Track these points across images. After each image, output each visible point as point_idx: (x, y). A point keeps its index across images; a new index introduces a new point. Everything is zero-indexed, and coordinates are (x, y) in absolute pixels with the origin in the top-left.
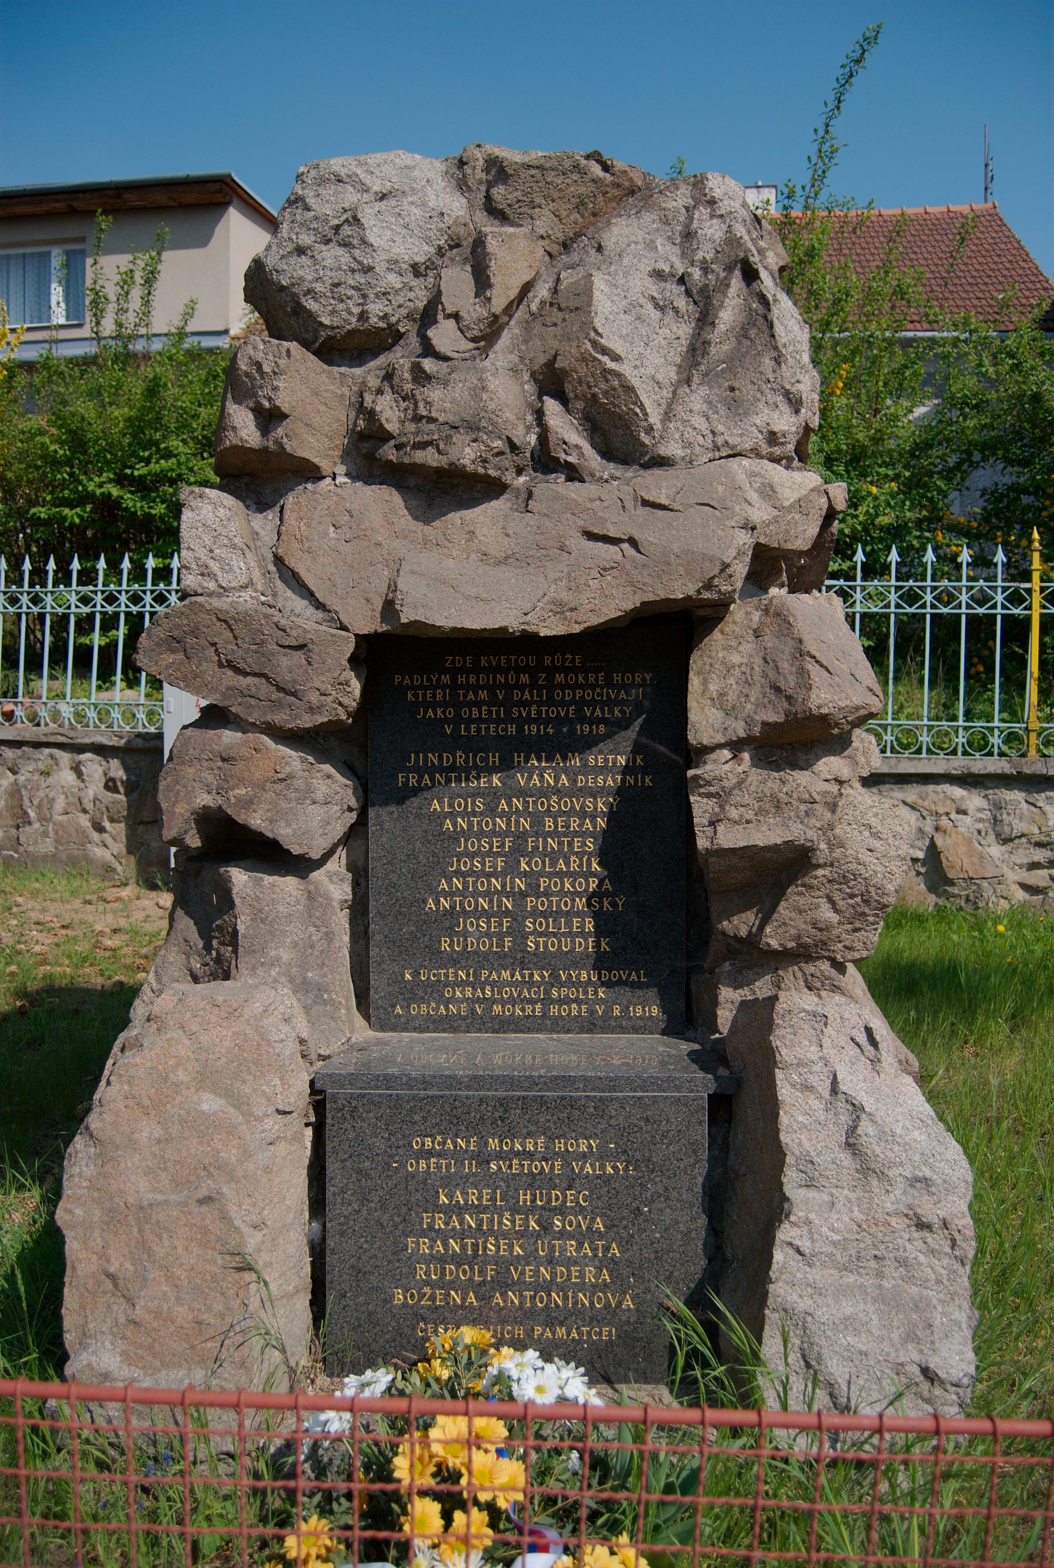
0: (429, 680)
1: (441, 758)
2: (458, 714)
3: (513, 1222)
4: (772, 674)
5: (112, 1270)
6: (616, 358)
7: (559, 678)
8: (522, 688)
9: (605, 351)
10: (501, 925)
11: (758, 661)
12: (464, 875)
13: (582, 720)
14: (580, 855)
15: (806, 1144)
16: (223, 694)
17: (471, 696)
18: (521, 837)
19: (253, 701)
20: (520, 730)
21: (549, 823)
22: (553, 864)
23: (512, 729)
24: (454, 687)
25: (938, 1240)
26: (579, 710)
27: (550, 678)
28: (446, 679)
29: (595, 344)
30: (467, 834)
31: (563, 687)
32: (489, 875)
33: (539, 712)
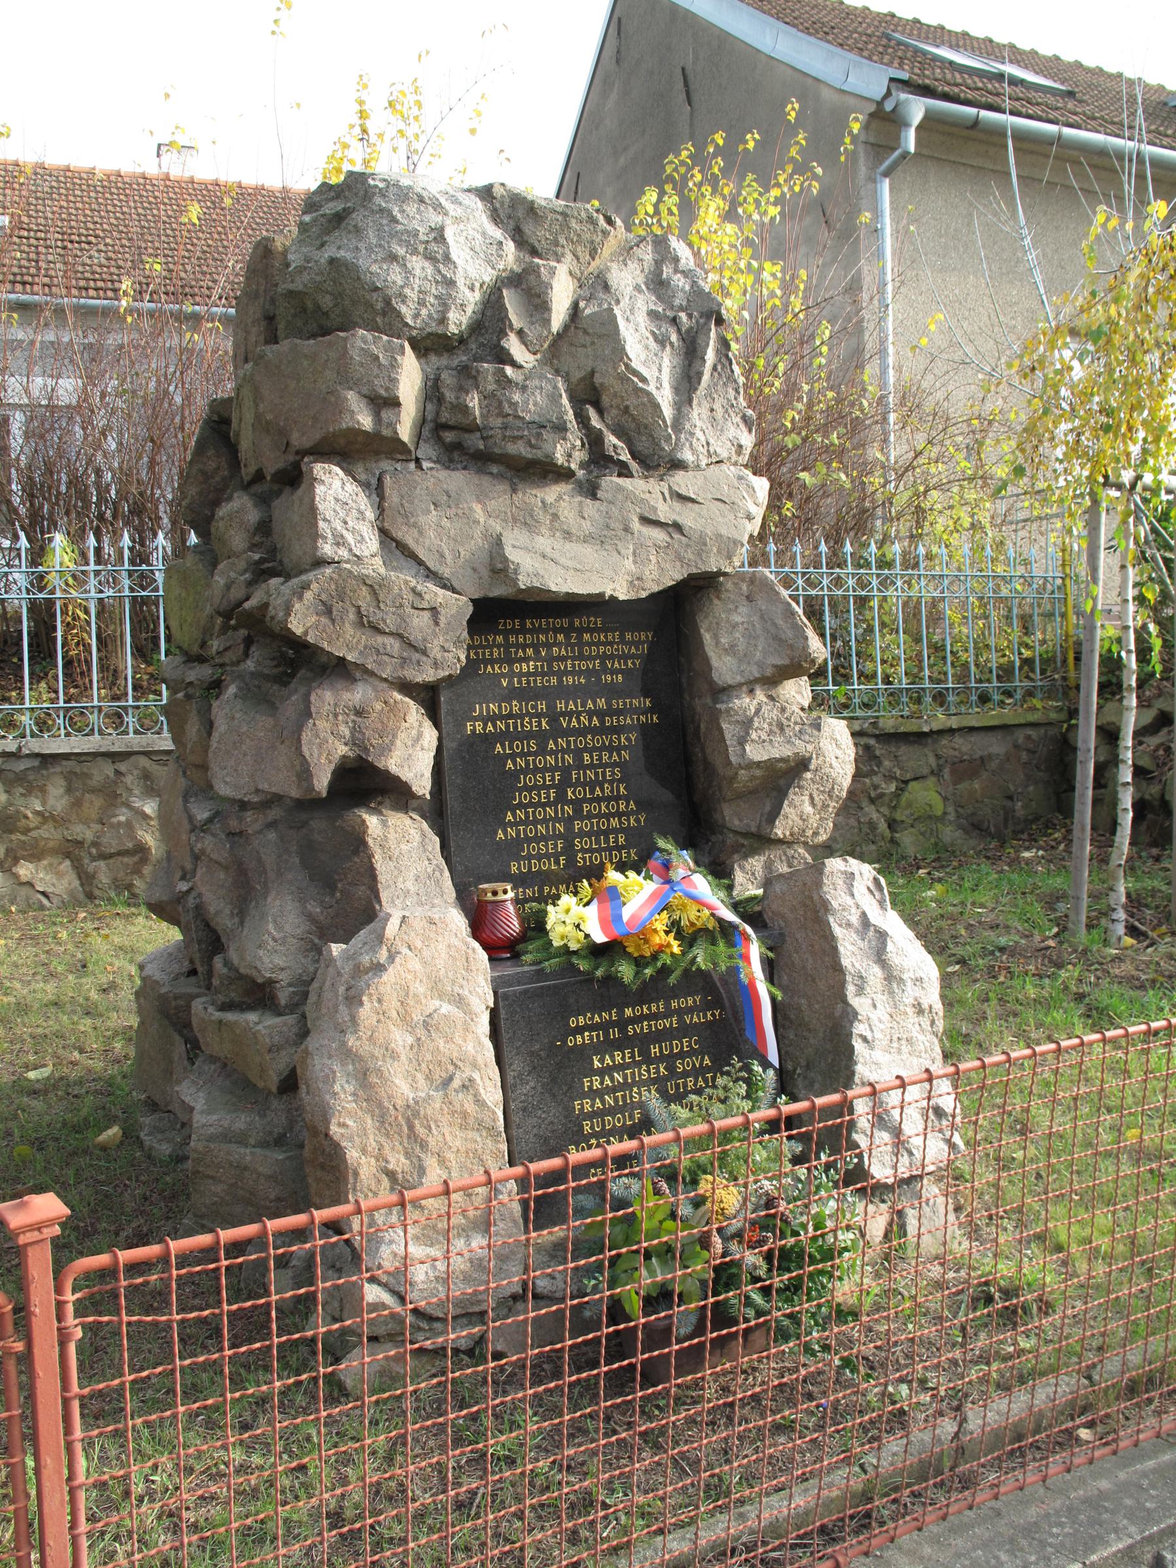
0: (487, 640)
1: (500, 707)
2: (511, 670)
3: (648, 1071)
4: (773, 630)
5: (391, 1167)
6: (644, 380)
7: (586, 637)
8: (559, 645)
9: (636, 373)
10: (556, 846)
11: (755, 618)
12: (526, 806)
13: (605, 670)
14: (611, 782)
15: (857, 965)
16: (361, 653)
17: (521, 654)
18: (566, 771)
19: (386, 658)
20: (560, 681)
21: (586, 757)
22: (592, 792)
23: (554, 681)
24: (507, 646)
25: (925, 1022)
26: (603, 663)
27: (580, 637)
28: (500, 639)
29: (627, 366)
30: (525, 771)
31: (590, 645)
32: (544, 805)
33: (573, 666)
